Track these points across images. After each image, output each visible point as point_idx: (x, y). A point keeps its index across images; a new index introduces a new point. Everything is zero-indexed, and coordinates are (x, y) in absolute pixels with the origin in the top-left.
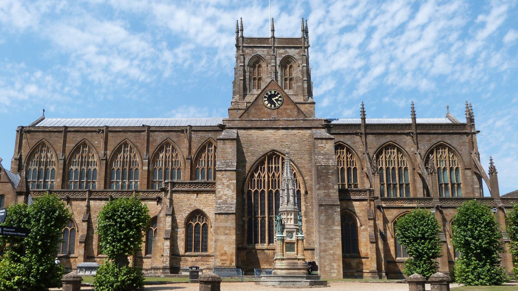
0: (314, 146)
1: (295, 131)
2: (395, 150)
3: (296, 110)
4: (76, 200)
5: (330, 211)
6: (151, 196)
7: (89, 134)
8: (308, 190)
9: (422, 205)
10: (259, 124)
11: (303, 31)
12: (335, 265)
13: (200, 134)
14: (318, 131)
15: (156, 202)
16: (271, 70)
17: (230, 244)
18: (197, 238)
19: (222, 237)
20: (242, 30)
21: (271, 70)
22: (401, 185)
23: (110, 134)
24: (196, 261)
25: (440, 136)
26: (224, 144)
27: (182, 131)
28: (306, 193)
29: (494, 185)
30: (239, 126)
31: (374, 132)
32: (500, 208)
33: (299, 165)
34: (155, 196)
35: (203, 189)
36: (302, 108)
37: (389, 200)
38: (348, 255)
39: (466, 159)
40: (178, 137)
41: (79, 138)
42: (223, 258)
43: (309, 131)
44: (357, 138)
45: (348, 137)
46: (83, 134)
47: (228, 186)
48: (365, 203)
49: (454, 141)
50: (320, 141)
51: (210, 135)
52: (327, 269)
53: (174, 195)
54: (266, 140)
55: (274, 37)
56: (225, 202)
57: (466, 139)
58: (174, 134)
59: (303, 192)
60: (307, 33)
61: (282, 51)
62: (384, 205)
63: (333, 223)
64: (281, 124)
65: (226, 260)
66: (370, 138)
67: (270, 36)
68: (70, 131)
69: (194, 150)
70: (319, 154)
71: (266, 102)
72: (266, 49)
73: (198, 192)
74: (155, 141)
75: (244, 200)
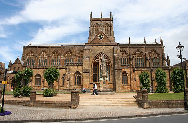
0: (113, 51)
1: (108, 47)
2: (140, 53)
3: (108, 40)
4: (41, 69)
5: (119, 71)
6: (63, 67)
7: (45, 48)
8: (112, 65)
9: (147, 69)
10: (97, 45)
11: (111, 16)
12: (120, 88)
14: (115, 46)
15: (65, 69)
16: (101, 27)
17: (88, 82)
18: (78, 80)
19: (85, 80)
20: (92, 16)
21: (101, 27)
22: (141, 63)
23: (51, 48)
24: (77, 87)
25: (153, 48)
26: (86, 51)
27: (73, 47)
28: (111, 66)
29: (168, 63)
30: (90, 45)
31: (133, 47)
32: (171, 70)
33: (109, 57)
34: (65, 67)
35: (79, 65)
36: (111, 39)
37: (137, 68)
38: (124, 85)
39: (161, 55)
41: (42, 49)
42: (86, 86)
43: (112, 47)
44: (128, 49)
45: (125, 48)
46: (43, 48)
47: (87, 64)
48: (130, 69)
49: (157, 50)
50: (116, 50)
51: (82, 48)
52: (118, 89)
53: (70, 67)
54: (99, 49)
55: (101, 18)
56: (86, 69)
57: (161, 49)
58: (71, 48)
59: (110, 65)
60: (112, 16)
61: (104, 22)
62: (136, 69)
63: (120, 75)
64: (104, 44)
65: (86, 87)
66: (132, 49)
67: (101, 17)
69: (77, 53)
70: (116, 54)
71: (99, 38)
72: (99, 21)
73: (78, 66)
74: (65, 50)
75: (92, 68)
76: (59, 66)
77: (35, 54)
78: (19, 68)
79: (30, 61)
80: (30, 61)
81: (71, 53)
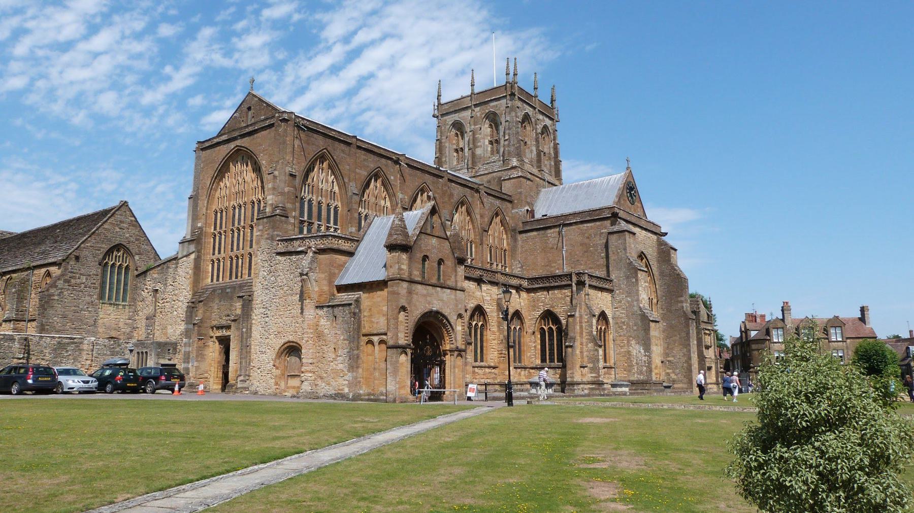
1: (650, 235)
13: (491, 199)
40: (473, 196)
41: (372, 163)
42: (657, 371)
43: (655, 237)
46: (377, 158)
61: (541, 117)
68: (359, 147)
69: (486, 220)
74: (451, 195)
76: (499, 275)
77: (346, 180)
78: (440, 262)
79: (315, 210)
80: (315, 210)
81: (469, 214)
